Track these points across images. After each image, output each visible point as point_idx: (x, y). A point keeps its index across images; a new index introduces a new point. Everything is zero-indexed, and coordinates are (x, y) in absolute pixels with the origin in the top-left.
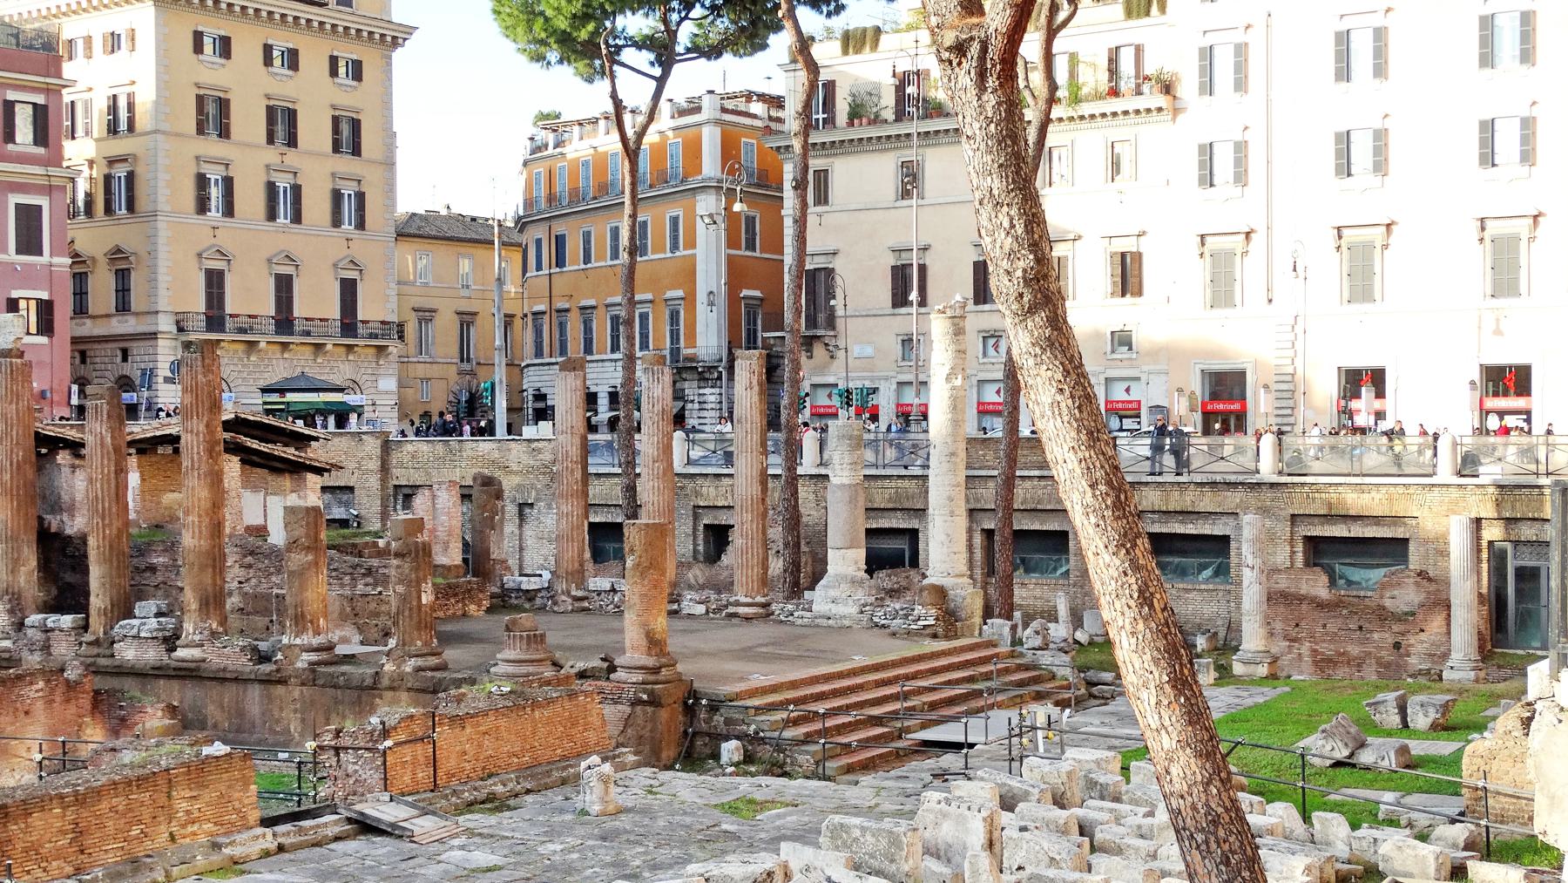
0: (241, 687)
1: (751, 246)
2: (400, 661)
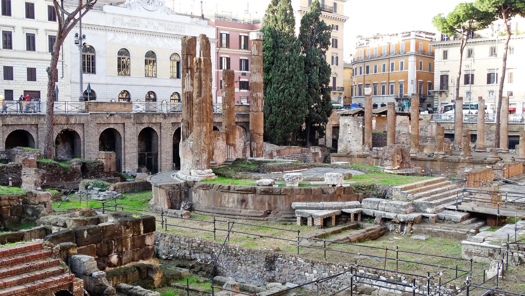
0: (425, 162)
1: (421, 69)
2: (465, 157)
